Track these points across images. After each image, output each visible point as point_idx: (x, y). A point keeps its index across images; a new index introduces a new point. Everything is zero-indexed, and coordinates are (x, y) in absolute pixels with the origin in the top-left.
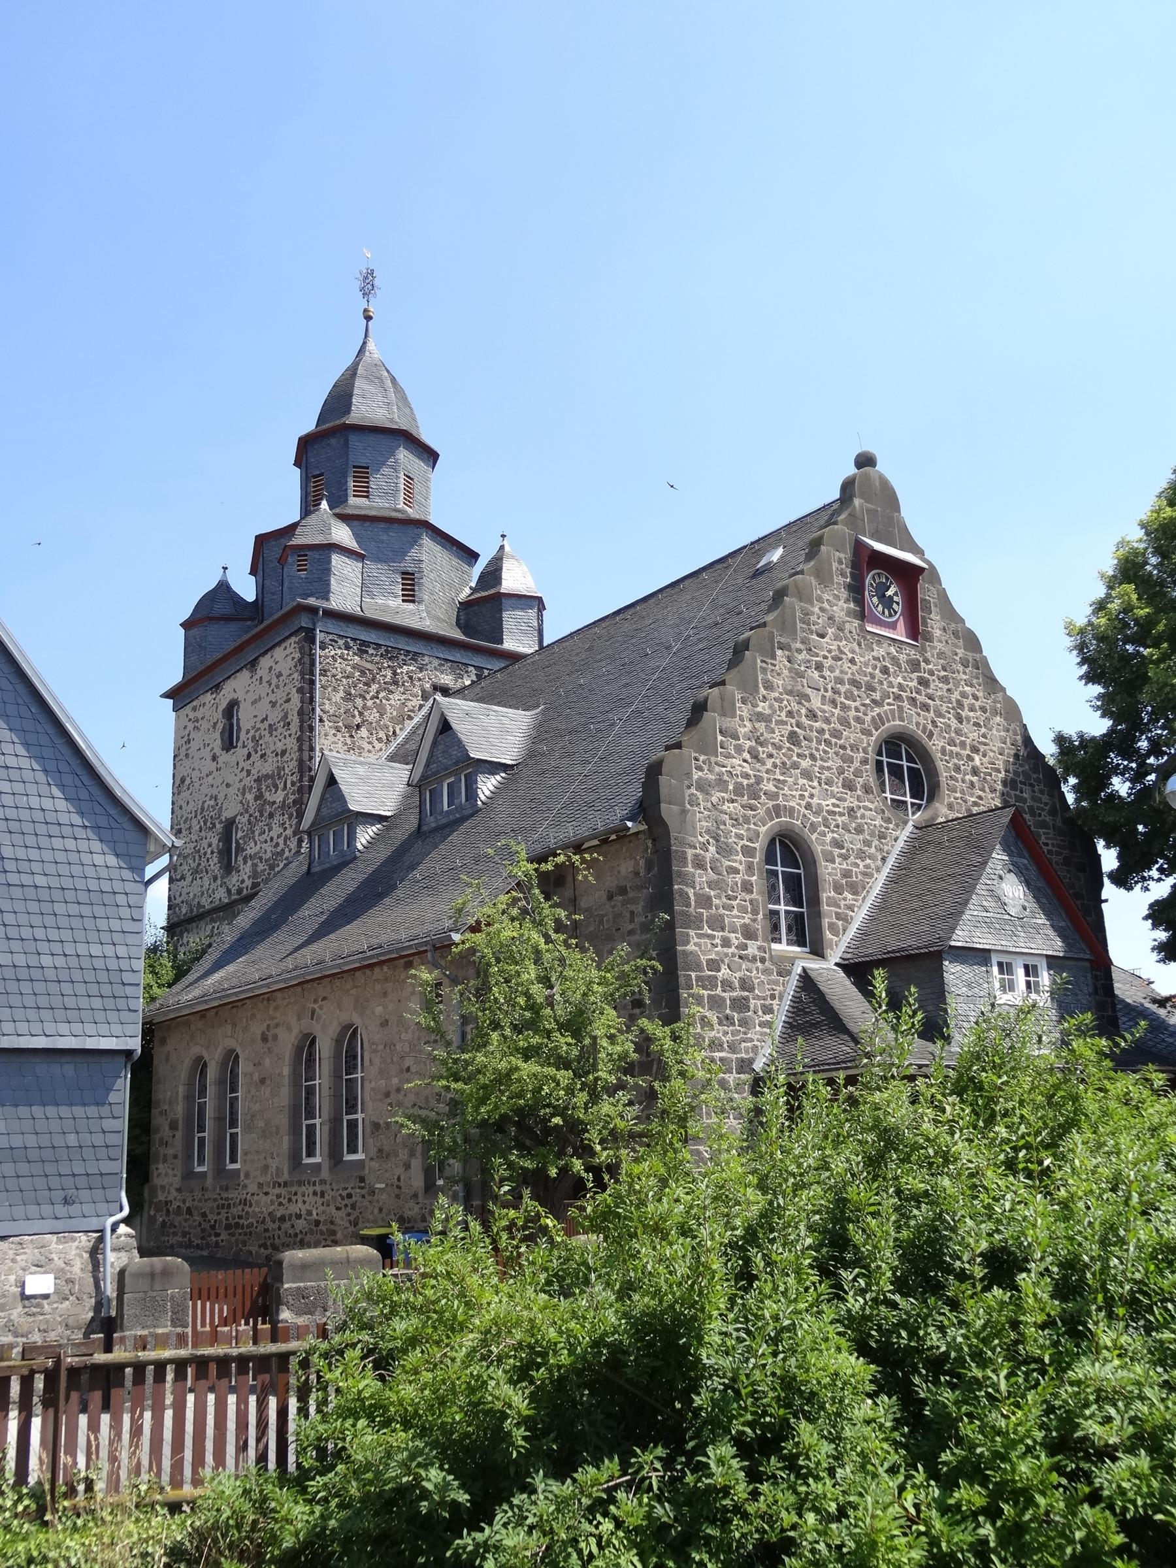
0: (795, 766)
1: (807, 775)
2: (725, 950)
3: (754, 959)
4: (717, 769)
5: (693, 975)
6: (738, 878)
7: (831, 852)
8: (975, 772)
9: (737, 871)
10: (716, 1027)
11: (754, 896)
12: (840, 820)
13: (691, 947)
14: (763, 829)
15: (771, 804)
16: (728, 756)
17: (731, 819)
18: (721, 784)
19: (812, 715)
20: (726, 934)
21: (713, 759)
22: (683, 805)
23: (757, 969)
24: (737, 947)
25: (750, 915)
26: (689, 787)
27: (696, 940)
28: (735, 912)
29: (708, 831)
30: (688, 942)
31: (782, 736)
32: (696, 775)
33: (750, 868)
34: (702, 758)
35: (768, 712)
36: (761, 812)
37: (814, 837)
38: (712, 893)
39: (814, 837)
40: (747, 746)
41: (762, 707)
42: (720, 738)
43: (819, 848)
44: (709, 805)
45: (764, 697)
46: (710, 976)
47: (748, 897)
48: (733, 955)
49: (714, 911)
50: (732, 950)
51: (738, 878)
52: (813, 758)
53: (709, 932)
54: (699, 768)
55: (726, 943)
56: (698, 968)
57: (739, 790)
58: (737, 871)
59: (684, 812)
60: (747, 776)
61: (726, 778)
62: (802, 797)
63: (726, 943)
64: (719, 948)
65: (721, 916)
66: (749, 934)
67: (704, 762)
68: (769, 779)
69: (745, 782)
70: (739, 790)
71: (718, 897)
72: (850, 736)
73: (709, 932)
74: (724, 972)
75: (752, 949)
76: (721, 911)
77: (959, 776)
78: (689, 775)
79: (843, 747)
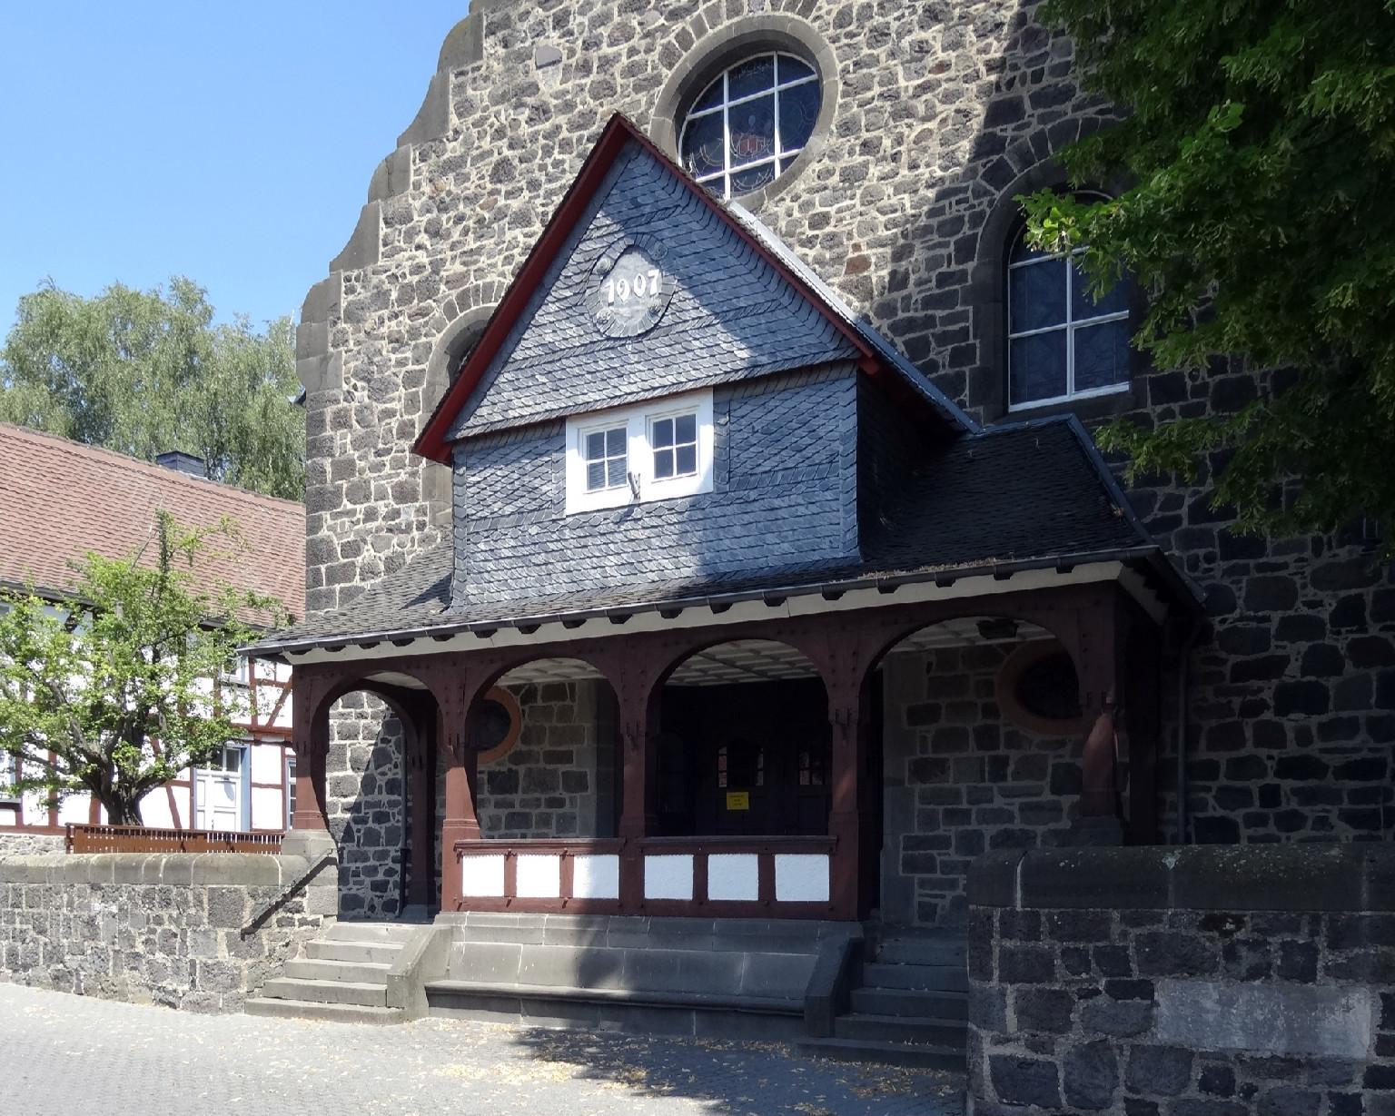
14: (437, 339)
17: (391, 342)
18: (381, 297)
19: (542, 112)
20: (372, 503)
28: (387, 470)
29: (355, 375)
38: (357, 454)
48: (378, 530)
52: (534, 185)
55: (371, 515)
71: (360, 458)
73: (350, 506)
74: (368, 553)
75: (409, 513)
76: (368, 474)
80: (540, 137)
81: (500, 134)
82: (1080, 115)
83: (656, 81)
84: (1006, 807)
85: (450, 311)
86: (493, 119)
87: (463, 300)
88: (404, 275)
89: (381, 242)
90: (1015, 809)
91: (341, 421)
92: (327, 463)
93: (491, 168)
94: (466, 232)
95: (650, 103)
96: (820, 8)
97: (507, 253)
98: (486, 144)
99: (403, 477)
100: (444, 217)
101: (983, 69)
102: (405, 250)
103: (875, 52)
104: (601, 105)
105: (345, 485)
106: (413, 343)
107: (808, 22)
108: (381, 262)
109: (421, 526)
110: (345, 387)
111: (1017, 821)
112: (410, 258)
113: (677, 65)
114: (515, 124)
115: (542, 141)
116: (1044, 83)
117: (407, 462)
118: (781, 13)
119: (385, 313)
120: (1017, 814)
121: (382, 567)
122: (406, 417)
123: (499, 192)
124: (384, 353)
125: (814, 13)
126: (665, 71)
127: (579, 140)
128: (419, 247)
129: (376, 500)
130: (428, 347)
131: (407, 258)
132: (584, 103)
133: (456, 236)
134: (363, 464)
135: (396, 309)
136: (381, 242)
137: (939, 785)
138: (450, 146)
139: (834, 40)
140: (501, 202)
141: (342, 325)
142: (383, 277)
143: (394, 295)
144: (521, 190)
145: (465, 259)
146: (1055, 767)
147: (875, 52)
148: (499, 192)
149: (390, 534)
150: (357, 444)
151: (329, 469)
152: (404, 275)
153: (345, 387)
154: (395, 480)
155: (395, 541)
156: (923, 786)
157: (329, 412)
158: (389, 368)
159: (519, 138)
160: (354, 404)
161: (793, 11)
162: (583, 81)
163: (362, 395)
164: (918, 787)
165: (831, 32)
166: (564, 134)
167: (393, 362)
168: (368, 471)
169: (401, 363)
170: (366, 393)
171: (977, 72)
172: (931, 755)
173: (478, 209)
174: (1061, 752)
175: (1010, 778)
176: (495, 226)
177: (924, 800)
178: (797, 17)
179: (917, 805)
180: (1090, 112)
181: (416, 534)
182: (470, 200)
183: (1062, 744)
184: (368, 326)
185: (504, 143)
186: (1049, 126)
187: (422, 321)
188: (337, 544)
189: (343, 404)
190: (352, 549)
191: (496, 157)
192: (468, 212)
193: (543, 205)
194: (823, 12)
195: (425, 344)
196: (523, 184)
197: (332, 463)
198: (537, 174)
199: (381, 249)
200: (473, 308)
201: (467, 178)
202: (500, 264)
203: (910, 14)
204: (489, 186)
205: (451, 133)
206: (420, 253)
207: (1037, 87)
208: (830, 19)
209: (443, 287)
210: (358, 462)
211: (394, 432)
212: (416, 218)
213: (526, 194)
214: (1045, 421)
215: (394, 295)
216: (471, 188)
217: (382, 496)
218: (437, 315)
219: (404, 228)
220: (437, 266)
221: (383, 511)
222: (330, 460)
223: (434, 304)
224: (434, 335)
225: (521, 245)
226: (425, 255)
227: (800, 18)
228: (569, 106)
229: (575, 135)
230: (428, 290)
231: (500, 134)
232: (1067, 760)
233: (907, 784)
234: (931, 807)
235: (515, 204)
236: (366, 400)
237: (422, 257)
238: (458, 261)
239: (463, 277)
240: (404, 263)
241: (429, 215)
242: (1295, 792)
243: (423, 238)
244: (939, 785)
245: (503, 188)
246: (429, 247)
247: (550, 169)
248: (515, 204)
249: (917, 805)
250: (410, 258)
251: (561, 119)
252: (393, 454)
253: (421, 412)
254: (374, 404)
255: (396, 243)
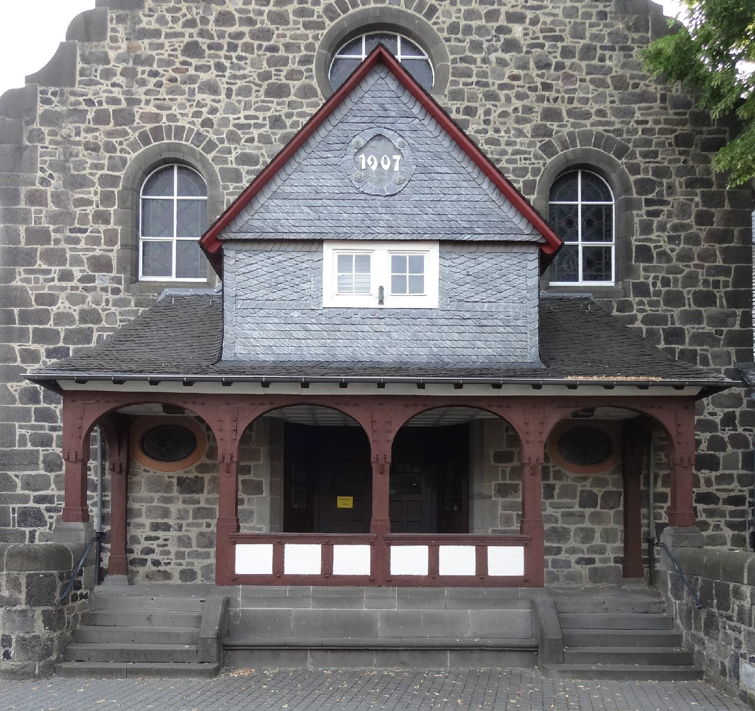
0: (192, 80)
1: (212, 88)
2: (64, 284)
3: (104, 290)
4: (72, 99)
5: (16, 311)
6: (90, 210)
7: (236, 169)
8: (511, 46)
9: (90, 203)
10: (43, 358)
11: (112, 226)
12: (255, 133)
13: (17, 283)
15: (148, 126)
16: (91, 83)
17: (87, 149)
18: (78, 115)
20: (68, 267)
21: (67, 89)
22: (19, 141)
23: (107, 302)
24: (79, 280)
25: (103, 247)
26: (28, 123)
27: (23, 276)
28: (82, 245)
29: (51, 166)
30: (13, 278)
31: (175, 50)
32: (41, 109)
33: (107, 199)
34: (52, 89)
35: (154, 26)
36: (134, 136)
37: (209, 157)
38: (52, 227)
39: (209, 157)
40: (119, 70)
41: (147, 23)
42: (79, 65)
43: (217, 168)
44: (58, 138)
45: (150, 10)
46: (38, 311)
47: (102, 227)
48: (73, 288)
49: (52, 245)
50: (75, 283)
51: (90, 210)
52: (220, 67)
53: (44, 267)
54: (47, 102)
55: (66, 276)
56: (25, 301)
57: (101, 118)
58: (90, 203)
59: (20, 149)
60: (114, 101)
61: (84, 107)
62: (197, 114)
63: (66, 276)
64: (56, 283)
65: (63, 251)
66: (101, 264)
67: (54, 94)
68: (148, 102)
69: (111, 108)
70: (101, 118)
71: (55, 231)
72: (281, 35)
74: (62, 305)
75: (102, 280)
76: (63, 245)
77: (478, 57)
78: (32, 109)
79: (273, 49)
80: (227, 36)
81: (191, 23)
82: (594, 128)
83: (321, 26)
84: (554, 514)
85: (144, 139)
86: (184, 10)
87: (157, 133)
88: (100, 103)
89: (78, 73)
90: (559, 515)
91: (36, 199)
92: (22, 229)
93: (182, 45)
94: (159, 85)
95: (316, 38)
96: (438, 18)
97: (196, 109)
98: (178, 28)
99: (98, 252)
100: (140, 69)
101: (540, 86)
102: (103, 84)
103: (475, 56)
104: (278, 29)
105: (40, 248)
106: (108, 155)
107: (430, 23)
108: (77, 88)
109: (116, 291)
110: (40, 174)
111: (560, 522)
112: (105, 91)
113: (337, 21)
114: (204, 20)
115: (227, 39)
116: (574, 105)
117: (103, 241)
118: (411, 11)
119: (83, 126)
120: (560, 518)
121: (77, 317)
122: (101, 208)
123: (190, 64)
124: (81, 155)
125: (434, 20)
126: (327, 22)
127: (260, 47)
128: (114, 85)
129: (71, 265)
130: (124, 161)
131: (102, 90)
132: (262, 22)
133: (151, 86)
134: (58, 236)
135: (92, 125)
136: (78, 73)
137: (513, 499)
138: (145, 19)
139: (448, 40)
140: (191, 71)
141: (36, 126)
142: (81, 99)
143: (90, 116)
144: (209, 68)
145: (158, 102)
146: (582, 491)
147: (475, 56)
148: (190, 64)
149: (85, 293)
150: (54, 218)
151: (23, 234)
152: (100, 103)
153: (40, 174)
154: (91, 254)
155: (89, 299)
156: (503, 499)
157: (24, 190)
158: (84, 169)
159: (207, 31)
160: (50, 190)
161: (420, 12)
162: (263, 8)
163: (56, 184)
164: (501, 500)
165: (445, 34)
166: (247, 39)
167: (89, 165)
168: (63, 242)
169: (96, 166)
170: (61, 182)
171: (537, 87)
172: (508, 482)
173: (170, 71)
174: (584, 483)
175: (556, 497)
176: (186, 87)
177: (504, 508)
178: (422, 18)
179: (500, 511)
180: (600, 129)
181: (110, 296)
182: (162, 63)
183: (585, 479)
184: (64, 132)
185: (194, 31)
186: (577, 130)
187: (118, 140)
188: (32, 294)
189: (38, 186)
190: (52, 300)
191: (187, 39)
192: (161, 70)
193: (227, 83)
194: (440, 21)
195: (121, 158)
196: (212, 63)
197: (27, 230)
198: (223, 60)
199: (78, 78)
200: (165, 141)
201: (161, 46)
202: (190, 115)
203: (496, 41)
204: (182, 58)
205: (146, 11)
206: (114, 89)
207: (570, 106)
208: (445, 26)
209: (137, 120)
210: (53, 234)
211: (90, 217)
212: (112, 63)
213: (213, 72)
214: (578, 295)
215: (90, 116)
216: (165, 54)
217: (77, 261)
218: (132, 138)
219: (100, 67)
220: (133, 102)
221: (77, 274)
222: (24, 226)
223: (129, 130)
224: (129, 153)
225: (209, 106)
226: (121, 92)
227: (424, 19)
228: (250, 22)
229: (256, 43)
230: (124, 117)
231: (191, 23)
232: (588, 488)
233: (493, 499)
234: (509, 512)
235: (204, 77)
236: (62, 189)
237: (117, 92)
238: (152, 103)
239: (156, 118)
240: (101, 94)
241: (125, 65)
242: (704, 510)
243: (119, 79)
244: (513, 499)
245: (194, 61)
246: (124, 87)
247: (234, 60)
248: (204, 77)
249: (500, 511)
250: (105, 91)
251: (246, 29)
252: (88, 234)
253: (116, 207)
254: (70, 193)
255: (93, 77)
